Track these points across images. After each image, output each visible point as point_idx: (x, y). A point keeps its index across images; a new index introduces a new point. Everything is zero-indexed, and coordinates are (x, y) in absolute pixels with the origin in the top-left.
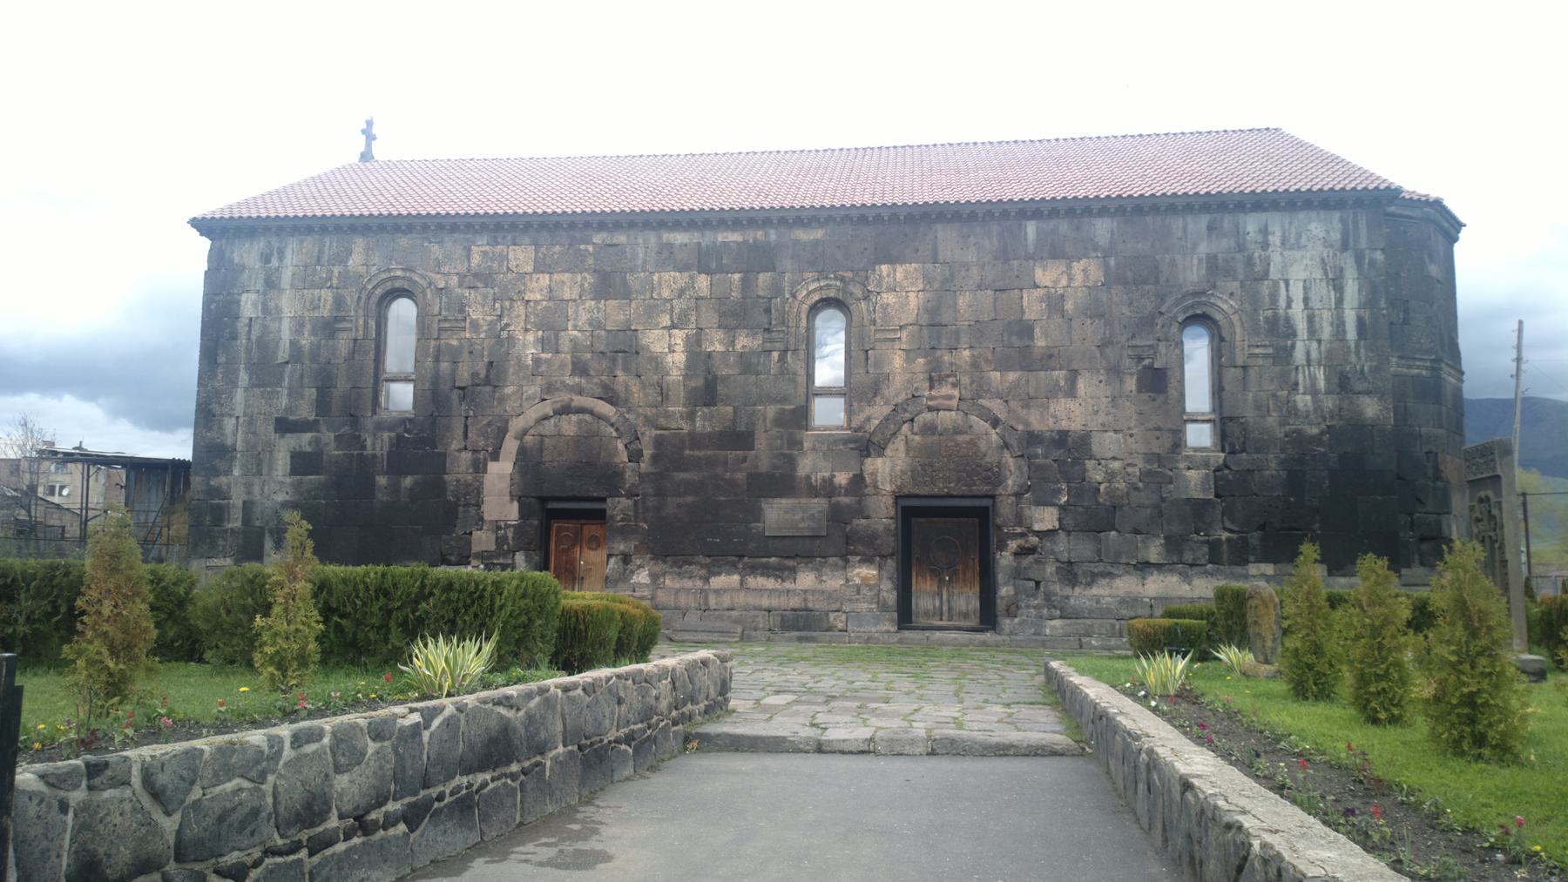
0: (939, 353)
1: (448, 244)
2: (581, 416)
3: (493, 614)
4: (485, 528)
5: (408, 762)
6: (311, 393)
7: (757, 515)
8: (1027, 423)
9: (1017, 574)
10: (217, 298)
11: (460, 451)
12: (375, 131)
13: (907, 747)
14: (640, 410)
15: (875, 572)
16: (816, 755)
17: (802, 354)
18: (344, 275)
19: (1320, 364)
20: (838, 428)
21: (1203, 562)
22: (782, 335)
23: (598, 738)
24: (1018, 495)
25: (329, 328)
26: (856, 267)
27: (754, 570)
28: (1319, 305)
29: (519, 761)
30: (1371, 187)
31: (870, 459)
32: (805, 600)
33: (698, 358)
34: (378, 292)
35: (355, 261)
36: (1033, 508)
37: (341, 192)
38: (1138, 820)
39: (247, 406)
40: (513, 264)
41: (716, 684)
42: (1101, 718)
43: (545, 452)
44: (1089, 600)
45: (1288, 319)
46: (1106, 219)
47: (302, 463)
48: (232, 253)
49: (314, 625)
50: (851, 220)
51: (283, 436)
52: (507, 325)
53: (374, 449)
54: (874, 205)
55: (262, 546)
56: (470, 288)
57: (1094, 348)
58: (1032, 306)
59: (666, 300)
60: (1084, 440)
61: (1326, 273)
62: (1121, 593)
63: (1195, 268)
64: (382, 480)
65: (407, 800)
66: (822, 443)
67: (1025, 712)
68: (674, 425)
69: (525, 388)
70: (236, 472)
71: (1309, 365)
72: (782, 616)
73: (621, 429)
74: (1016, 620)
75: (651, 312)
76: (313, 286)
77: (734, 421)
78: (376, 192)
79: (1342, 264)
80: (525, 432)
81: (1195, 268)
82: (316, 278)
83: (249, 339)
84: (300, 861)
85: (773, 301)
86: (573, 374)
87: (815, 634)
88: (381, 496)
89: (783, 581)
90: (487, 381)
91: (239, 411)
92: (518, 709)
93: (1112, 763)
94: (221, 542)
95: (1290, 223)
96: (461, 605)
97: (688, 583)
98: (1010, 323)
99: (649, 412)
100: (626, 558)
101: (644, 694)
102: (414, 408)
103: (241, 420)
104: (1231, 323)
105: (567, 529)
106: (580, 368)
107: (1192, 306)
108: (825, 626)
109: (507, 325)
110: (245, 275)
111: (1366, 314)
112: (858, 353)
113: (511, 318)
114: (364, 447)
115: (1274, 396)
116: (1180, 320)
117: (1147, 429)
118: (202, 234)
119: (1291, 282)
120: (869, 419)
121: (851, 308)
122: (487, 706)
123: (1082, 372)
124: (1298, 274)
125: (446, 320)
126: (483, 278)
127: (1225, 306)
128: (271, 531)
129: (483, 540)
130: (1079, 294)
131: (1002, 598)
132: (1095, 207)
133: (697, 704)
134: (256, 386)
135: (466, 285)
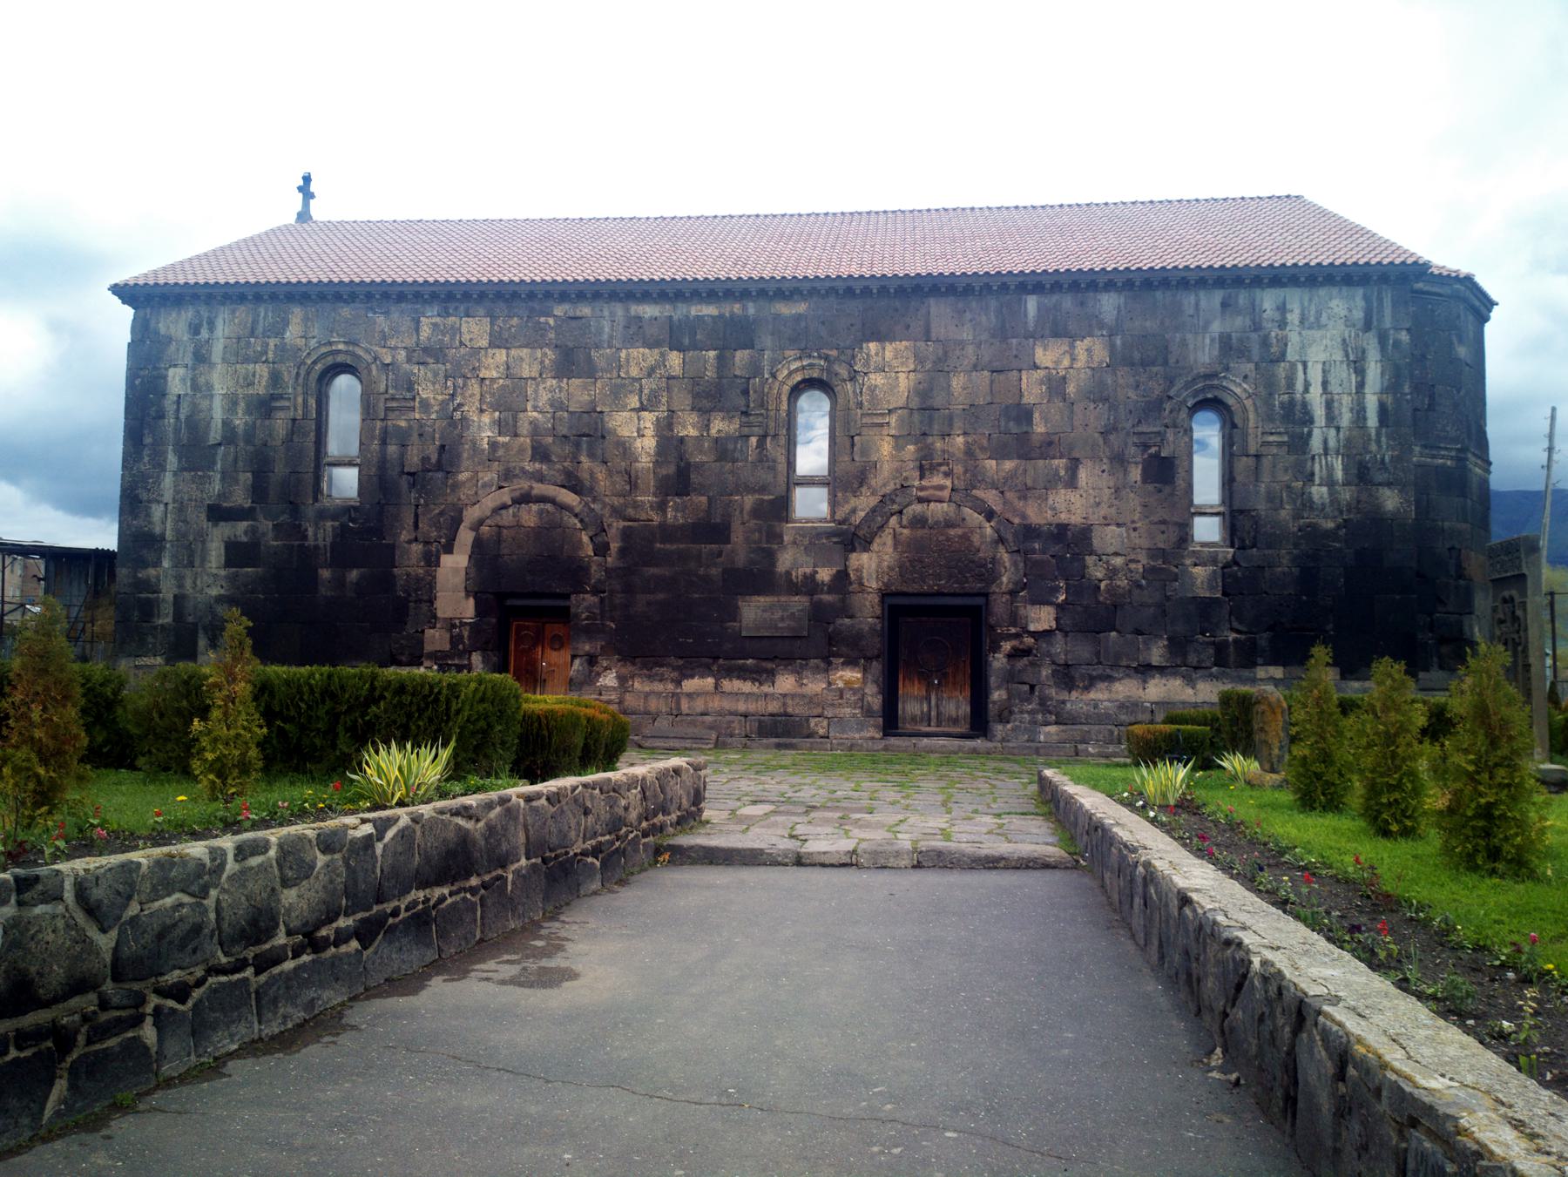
0: (930, 440)
1: (395, 316)
2: (542, 505)
3: (449, 718)
4: (438, 625)
5: (361, 876)
6: (246, 478)
7: (734, 614)
8: (1024, 516)
9: (1010, 678)
10: (142, 373)
11: (410, 542)
12: (313, 188)
13: (892, 860)
14: (607, 500)
15: (859, 675)
16: (795, 868)
17: (782, 441)
18: (282, 349)
19: (1338, 453)
20: (820, 521)
21: (1208, 664)
22: (760, 419)
23: (563, 851)
24: (1013, 593)
25: (265, 407)
26: (842, 344)
27: (730, 673)
28: (1339, 390)
29: (478, 875)
30: (1397, 261)
31: (854, 556)
32: (784, 704)
33: (669, 444)
34: (319, 367)
35: (293, 334)
36: (1029, 607)
37: (276, 257)
38: (1133, 936)
39: (177, 492)
40: (466, 338)
41: (689, 794)
42: (1096, 829)
43: (503, 545)
44: (1087, 705)
45: (1305, 404)
46: (1112, 294)
47: (237, 554)
49: (257, 730)
50: (837, 293)
51: (216, 525)
52: (460, 405)
53: (316, 540)
54: (862, 276)
55: (195, 644)
56: (418, 363)
57: (1097, 435)
58: (1031, 388)
59: (635, 380)
60: (1085, 533)
61: (1347, 356)
62: (1120, 697)
63: (1207, 349)
64: (325, 574)
65: (359, 916)
66: (804, 536)
67: (1017, 822)
68: (644, 517)
69: (480, 475)
70: (166, 564)
71: (1326, 454)
72: (760, 722)
73: (587, 519)
74: (1009, 726)
75: (617, 393)
76: (247, 360)
77: (708, 512)
78: (314, 256)
79: (1365, 345)
80: (481, 522)
81: (1207, 349)
82: (251, 352)
83: (177, 418)
84: (246, 980)
85: (752, 381)
86: (533, 459)
87: (795, 741)
88: (324, 591)
89: (761, 684)
90: (439, 467)
91: (168, 496)
92: (478, 820)
93: (1107, 875)
94: (150, 639)
95: (1310, 300)
96: (414, 708)
97: (658, 687)
98: (1007, 407)
99: (616, 501)
100: (592, 660)
101: (612, 804)
102: (360, 494)
103: (170, 507)
104: (1245, 409)
105: (527, 628)
106: (540, 453)
107: (1203, 390)
108: (805, 732)
109: (460, 405)
110: (173, 347)
111: (1389, 400)
112: (843, 439)
113: (464, 398)
114: (305, 537)
115: (1288, 487)
116: (1189, 404)
117: (1152, 523)
118: (124, 303)
119: (1310, 364)
120: (854, 511)
121: (836, 389)
122: (444, 817)
123: (1084, 461)
124: (1316, 356)
125: (393, 399)
126: (431, 353)
127: (1238, 389)
128: (205, 628)
129: (436, 639)
130: (1082, 376)
131: (994, 703)
132: (1102, 280)
133: (669, 814)
134: (183, 469)
135: (414, 360)
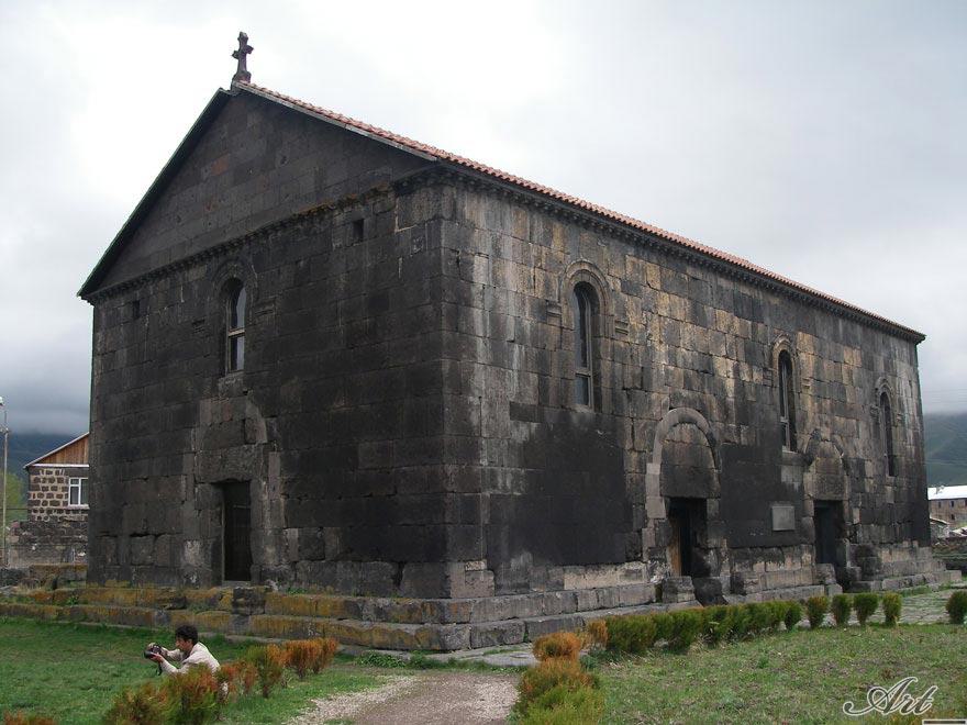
6: (534, 377)
18: (549, 255)
33: (740, 387)
35: (556, 244)
40: (650, 279)
48: (464, 206)
52: (650, 334)
75: (717, 341)
76: (526, 263)
134: (492, 364)
